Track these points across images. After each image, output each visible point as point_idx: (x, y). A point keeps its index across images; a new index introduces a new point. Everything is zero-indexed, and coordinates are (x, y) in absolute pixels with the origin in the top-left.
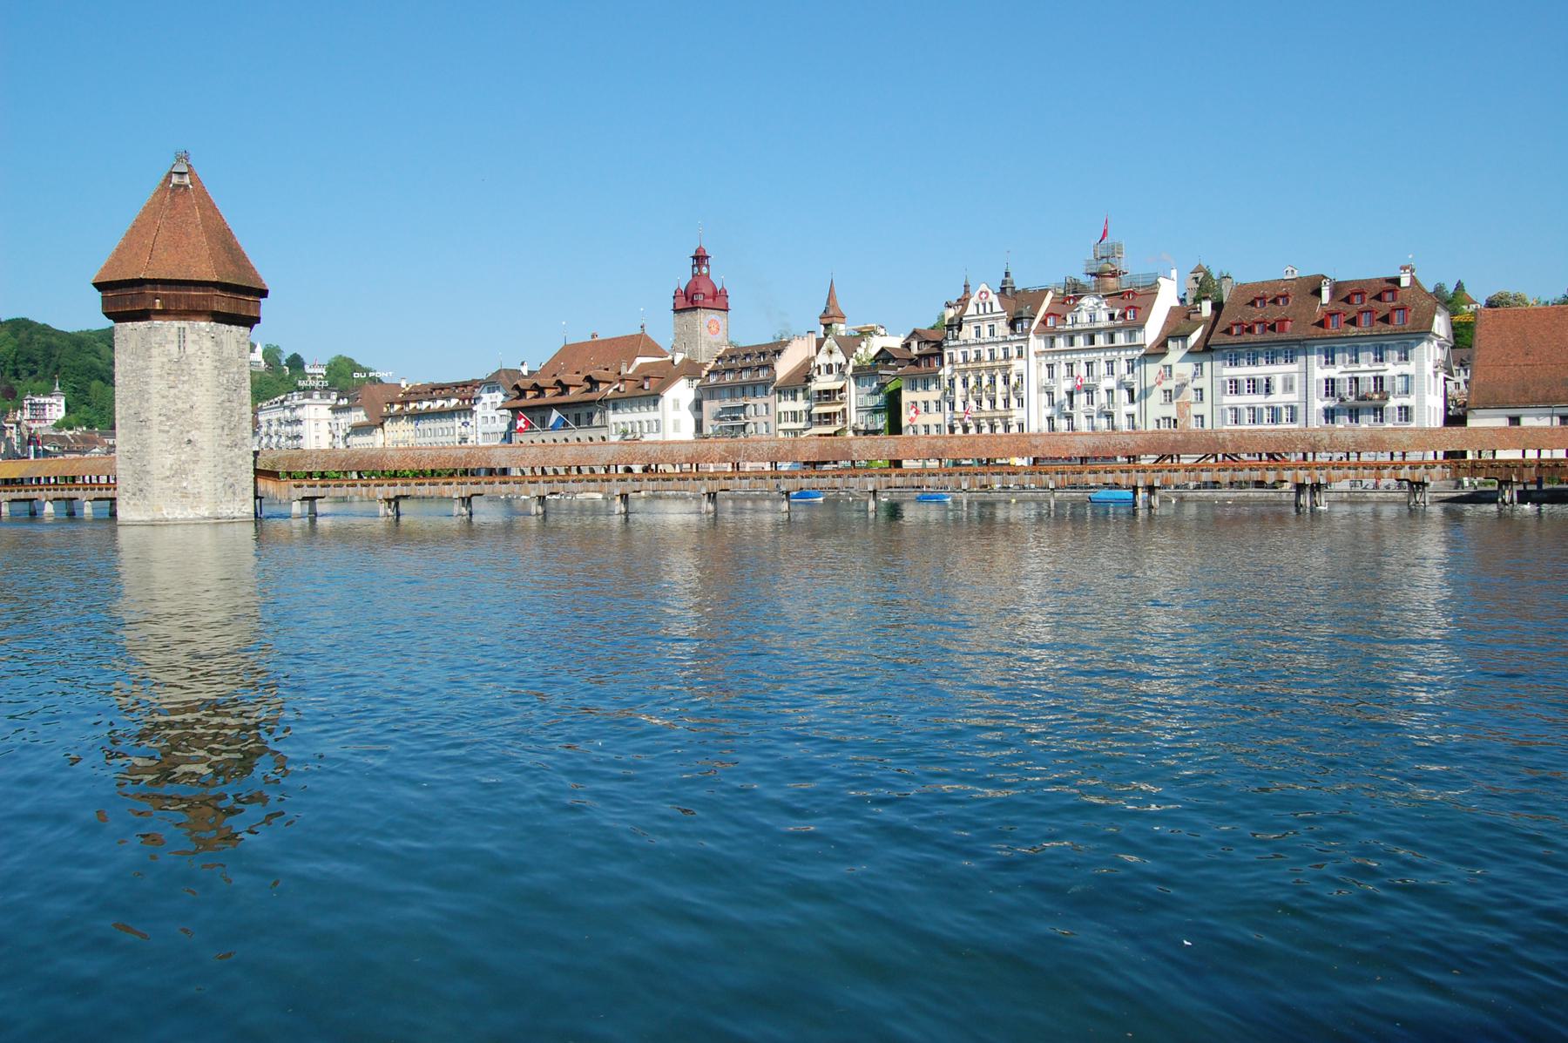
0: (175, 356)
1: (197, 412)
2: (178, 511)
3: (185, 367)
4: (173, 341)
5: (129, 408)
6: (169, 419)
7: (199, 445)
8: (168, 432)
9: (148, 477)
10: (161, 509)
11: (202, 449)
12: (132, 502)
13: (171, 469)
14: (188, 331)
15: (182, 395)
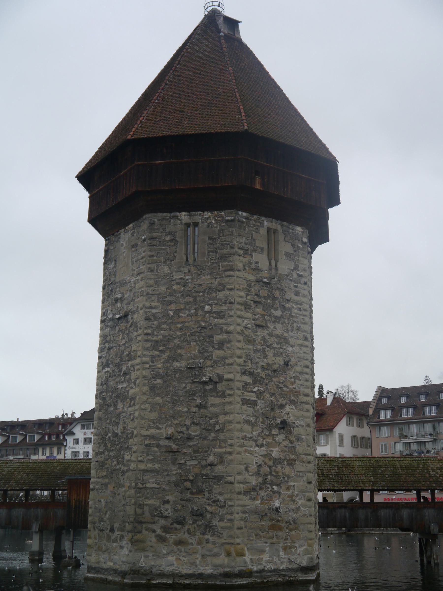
0: (265, 274)
1: (291, 373)
2: (266, 557)
3: (277, 294)
4: (262, 249)
5: (176, 358)
6: (257, 380)
7: (296, 431)
8: (254, 404)
9: (217, 488)
10: (241, 554)
11: (299, 439)
12: (172, 537)
13: (258, 474)
14: (281, 237)
15: (273, 340)
